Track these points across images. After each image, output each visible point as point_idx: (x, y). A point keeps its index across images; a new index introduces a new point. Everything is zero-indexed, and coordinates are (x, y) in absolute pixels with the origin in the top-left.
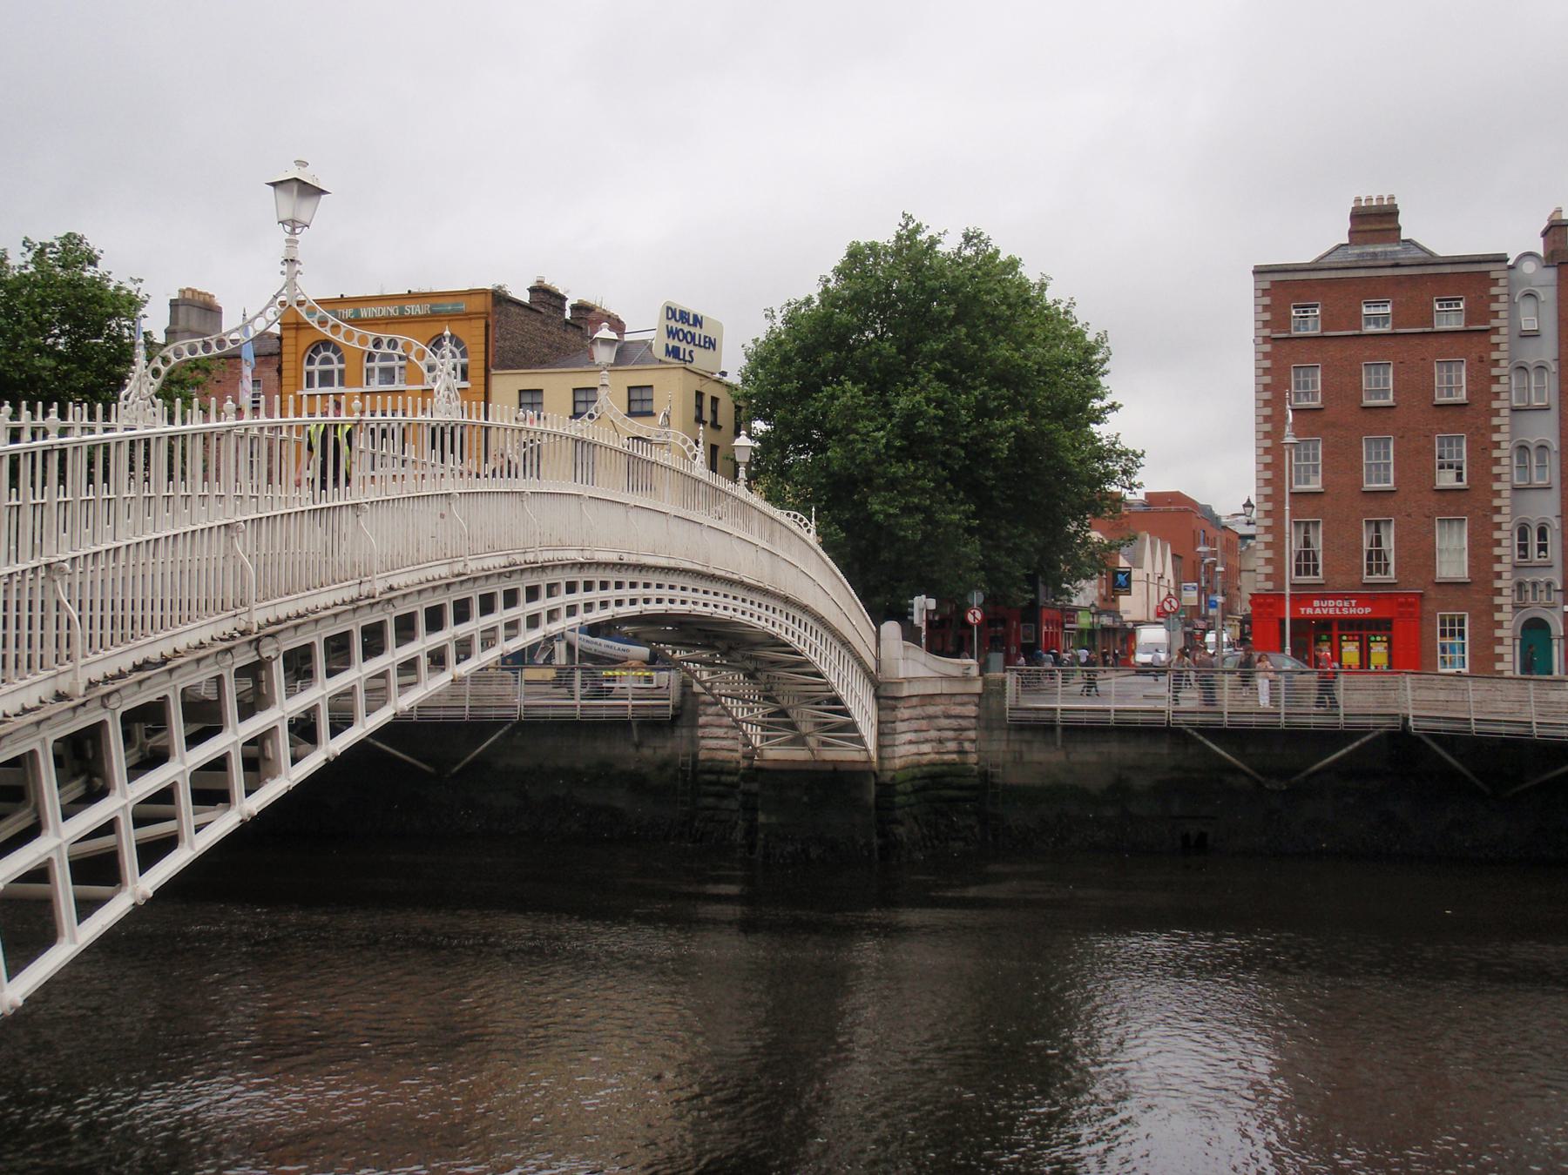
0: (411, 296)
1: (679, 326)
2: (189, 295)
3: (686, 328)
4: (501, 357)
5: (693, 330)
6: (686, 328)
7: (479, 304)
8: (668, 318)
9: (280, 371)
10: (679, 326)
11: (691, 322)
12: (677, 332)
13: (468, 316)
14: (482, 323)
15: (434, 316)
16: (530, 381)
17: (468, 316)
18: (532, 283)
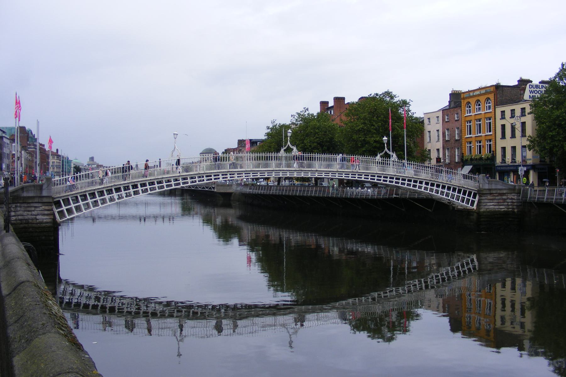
0: (480, 89)
1: (535, 89)
2: (453, 92)
3: (538, 90)
4: (498, 103)
5: (541, 90)
6: (538, 90)
7: (492, 89)
8: (530, 88)
9: (461, 110)
10: (533, 89)
11: (540, 87)
12: (534, 91)
13: (491, 92)
14: (493, 94)
15: (486, 93)
16: (503, 109)
17: (491, 92)
18: (519, 79)
